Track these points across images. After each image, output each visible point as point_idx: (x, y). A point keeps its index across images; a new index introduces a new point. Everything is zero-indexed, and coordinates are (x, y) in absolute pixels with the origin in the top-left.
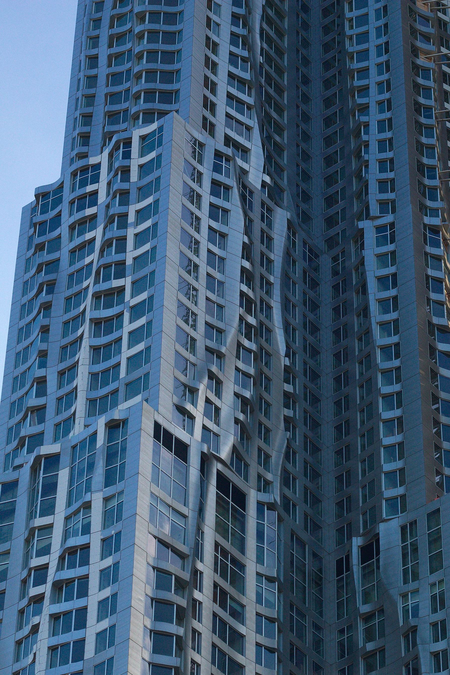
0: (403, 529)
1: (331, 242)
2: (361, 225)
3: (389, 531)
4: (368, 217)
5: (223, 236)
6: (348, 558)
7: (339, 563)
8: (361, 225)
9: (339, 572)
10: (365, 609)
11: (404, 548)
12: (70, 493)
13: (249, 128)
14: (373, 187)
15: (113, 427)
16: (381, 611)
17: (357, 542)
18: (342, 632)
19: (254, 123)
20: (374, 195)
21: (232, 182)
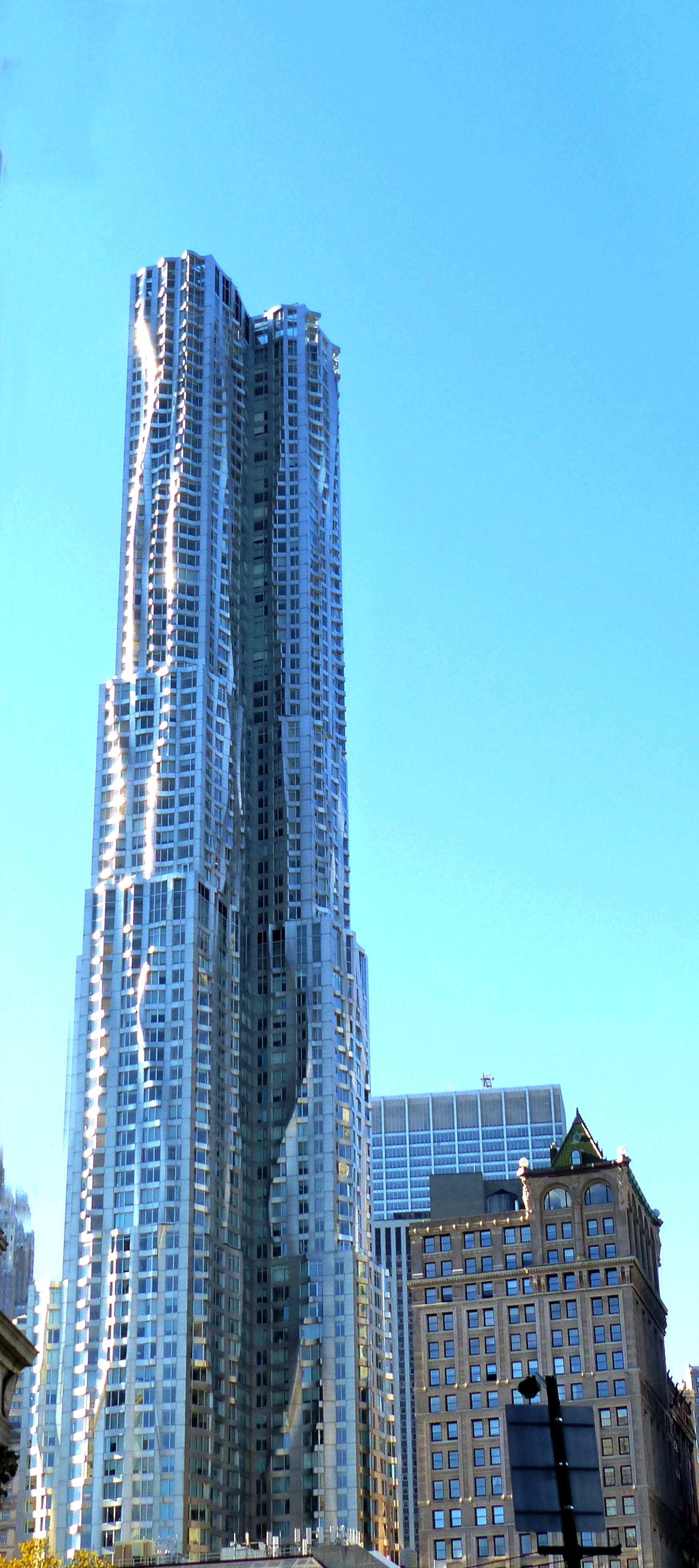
0: (298, 928)
1: (258, 718)
2: (280, 718)
3: (290, 927)
4: (284, 714)
5: (221, 742)
6: (266, 934)
7: (260, 935)
8: (280, 718)
9: (260, 941)
10: (276, 970)
11: (299, 940)
12: (151, 914)
13: (227, 652)
14: (287, 694)
15: (177, 881)
16: (284, 974)
17: (271, 927)
18: (260, 978)
19: (229, 648)
20: (288, 701)
21: (225, 705)
